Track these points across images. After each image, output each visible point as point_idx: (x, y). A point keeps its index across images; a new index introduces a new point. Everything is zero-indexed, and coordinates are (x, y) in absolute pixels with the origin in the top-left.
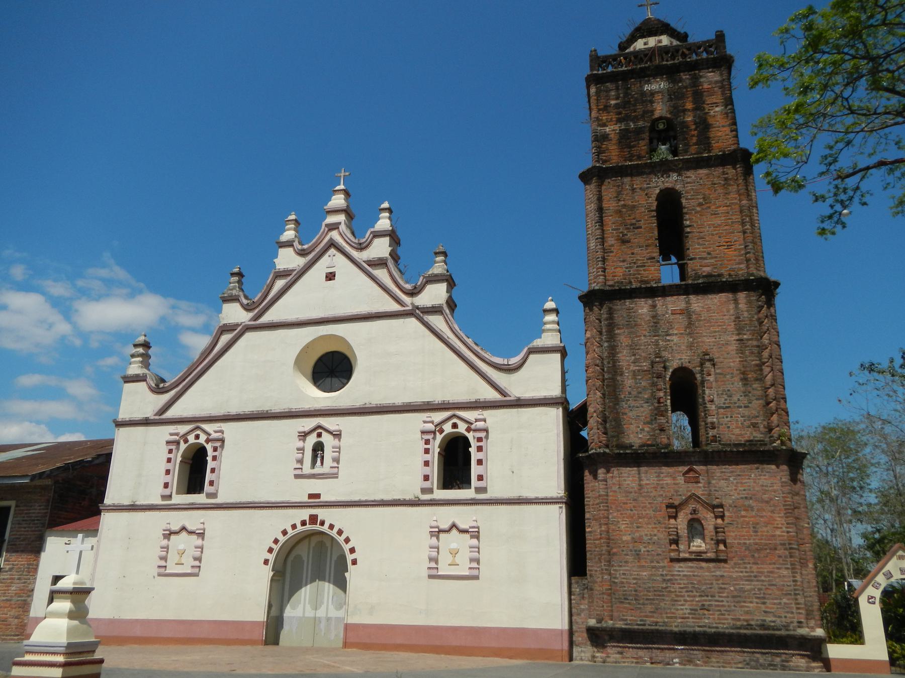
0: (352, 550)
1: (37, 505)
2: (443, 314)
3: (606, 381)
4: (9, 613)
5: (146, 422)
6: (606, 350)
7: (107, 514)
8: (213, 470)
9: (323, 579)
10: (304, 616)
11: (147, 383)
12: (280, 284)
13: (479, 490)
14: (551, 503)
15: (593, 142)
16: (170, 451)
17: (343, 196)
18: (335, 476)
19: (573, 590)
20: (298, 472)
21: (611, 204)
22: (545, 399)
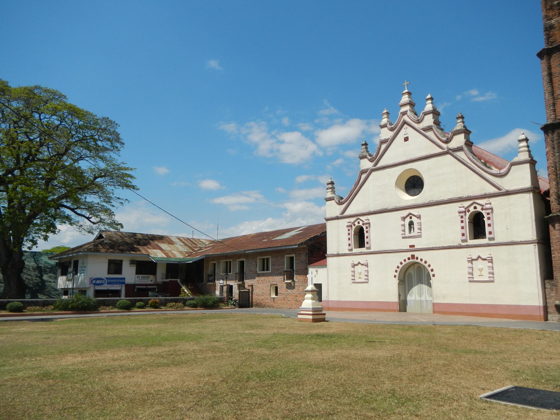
0: (432, 270)
2: (463, 151)
3: (558, 175)
5: (337, 218)
6: (557, 158)
8: (367, 237)
9: (422, 283)
10: (416, 300)
12: (384, 146)
13: (490, 239)
14: (529, 243)
15: (544, 32)
16: (349, 230)
17: (407, 96)
18: (420, 236)
19: (546, 286)
20: (404, 236)
21: (557, 69)
22: (522, 189)
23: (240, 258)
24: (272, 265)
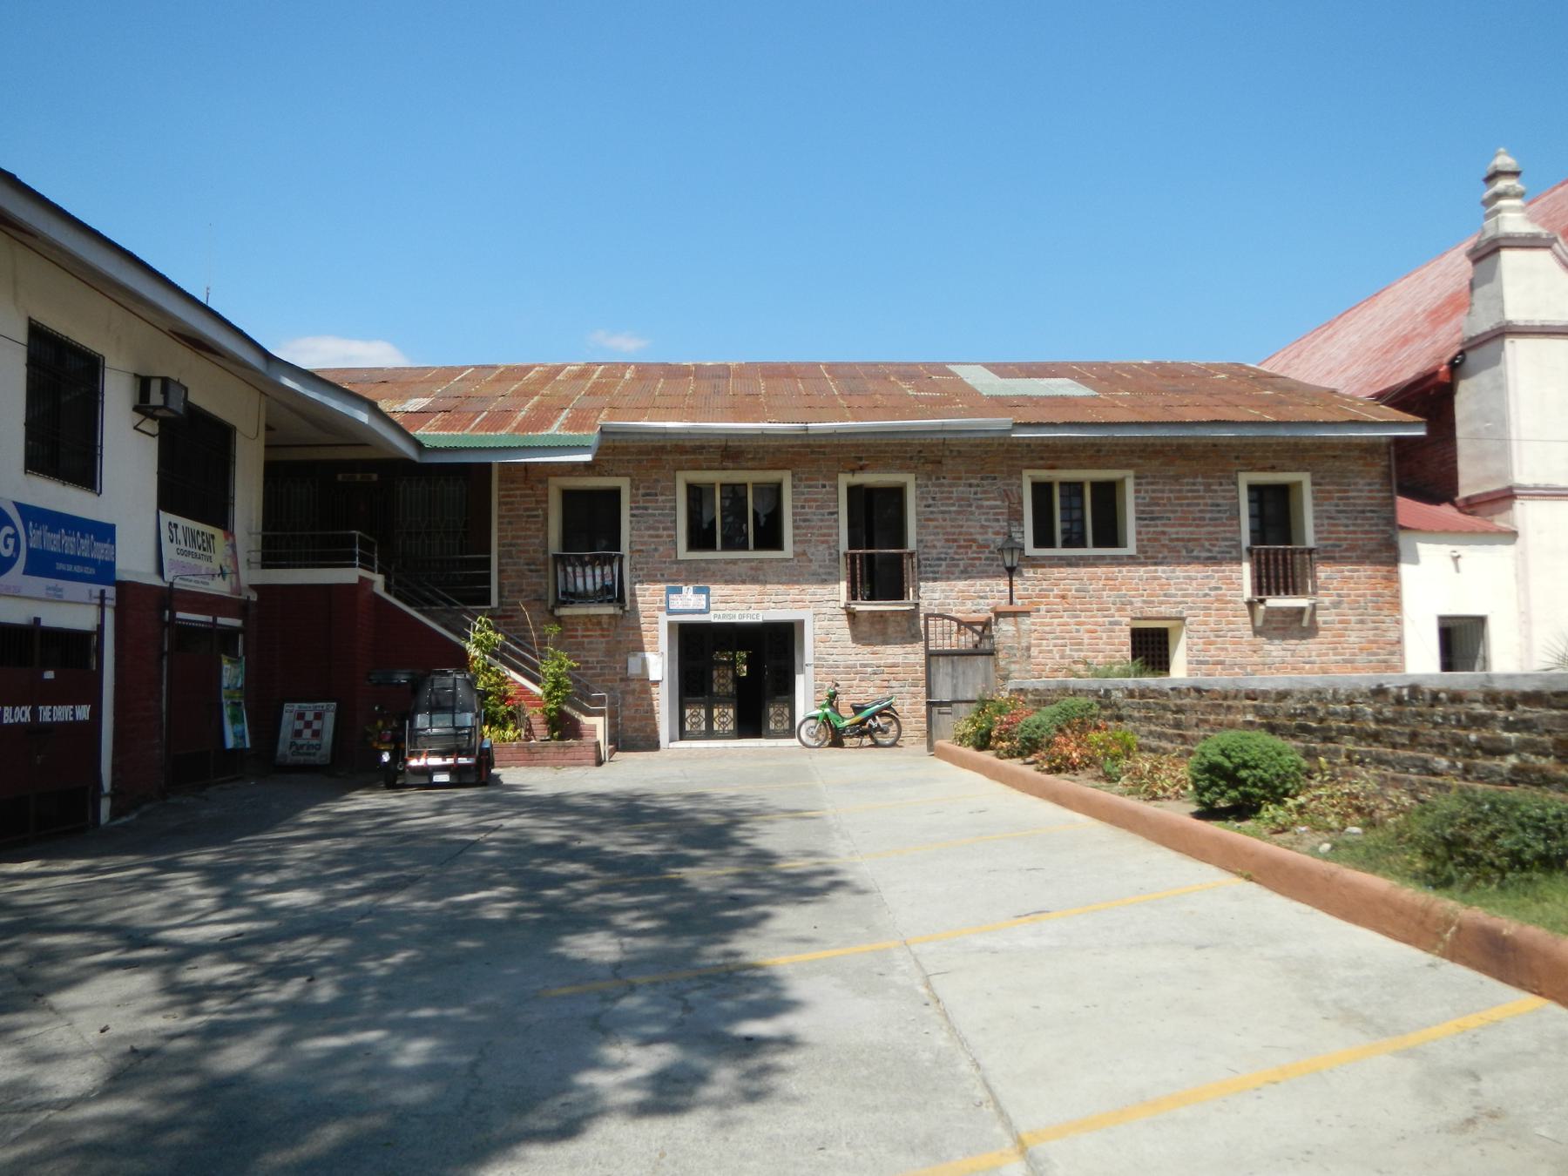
11: (1555, 253)
23: (862, 468)
24: (1138, 519)
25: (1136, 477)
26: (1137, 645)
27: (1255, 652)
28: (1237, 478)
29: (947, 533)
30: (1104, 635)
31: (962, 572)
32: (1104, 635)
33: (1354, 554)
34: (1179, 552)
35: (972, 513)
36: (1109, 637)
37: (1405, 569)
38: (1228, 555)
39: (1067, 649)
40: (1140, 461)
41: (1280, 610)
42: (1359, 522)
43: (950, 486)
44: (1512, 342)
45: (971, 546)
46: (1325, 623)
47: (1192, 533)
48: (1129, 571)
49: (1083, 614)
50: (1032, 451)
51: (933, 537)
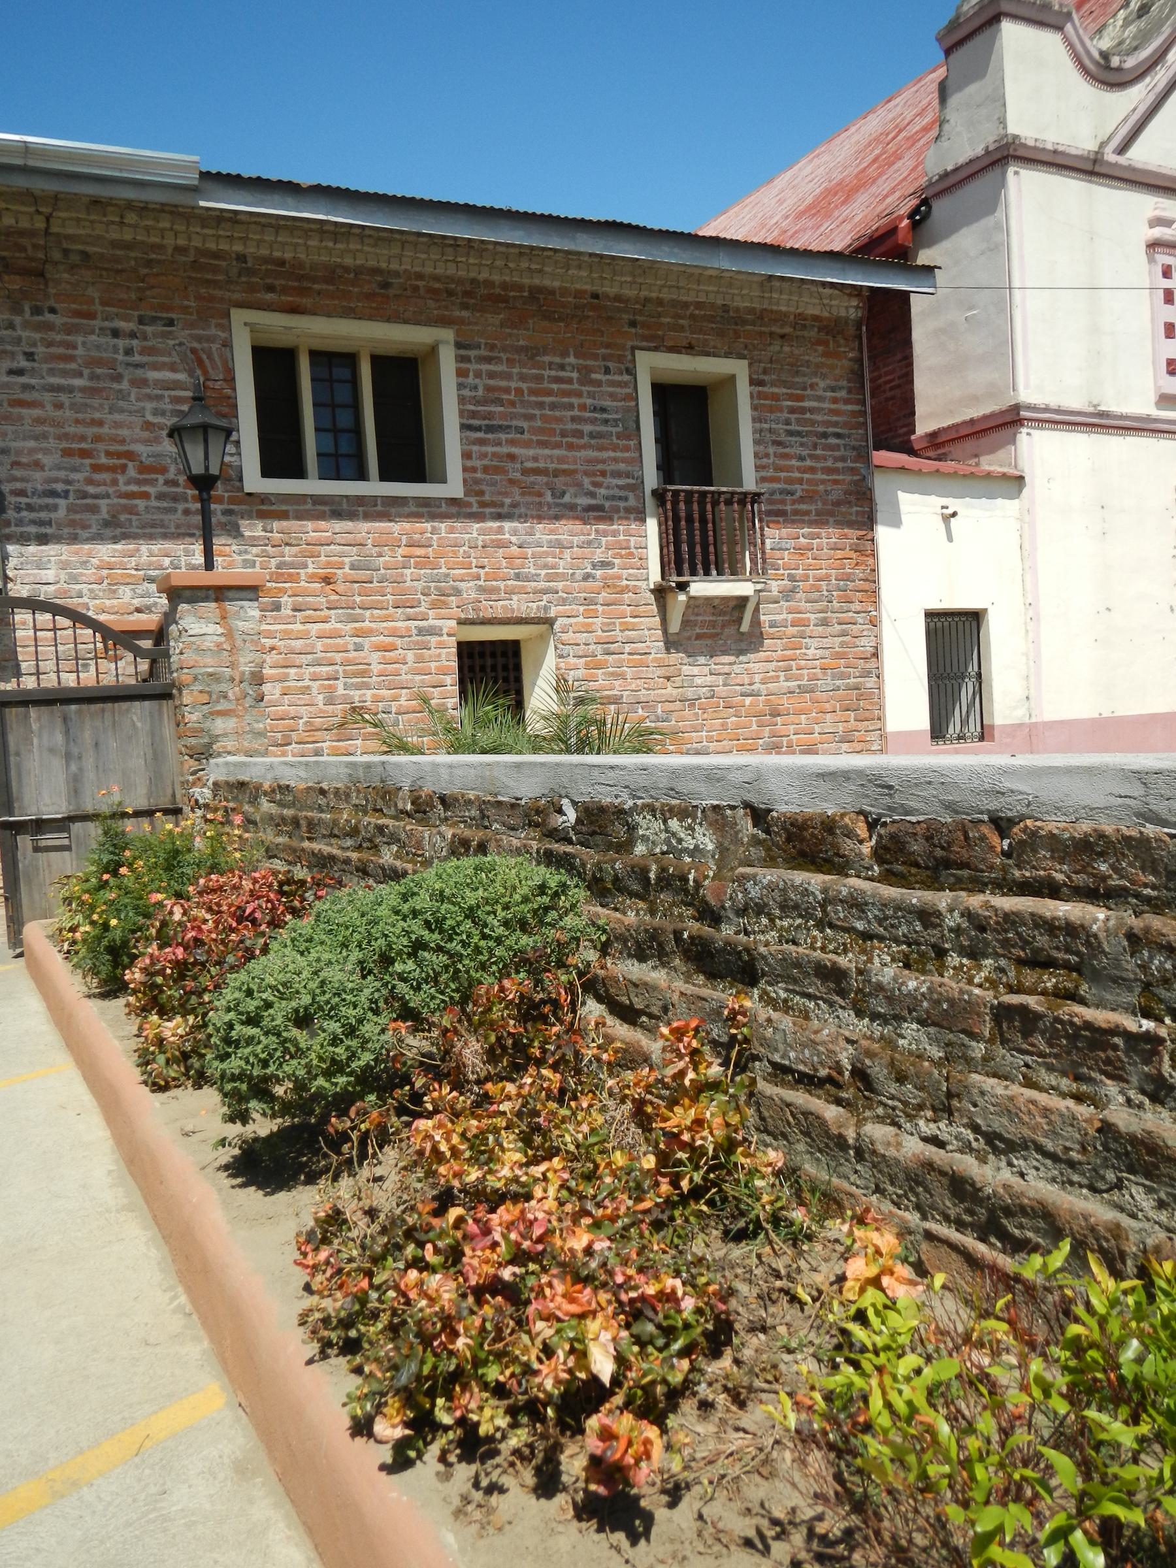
1: (822, 384)
4: (817, 728)
7: (1036, 433)
11: (1066, 39)
24: (464, 427)
25: (459, 345)
26: (467, 675)
27: (668, 679)
28: (634, 361)
29: (66, 437)
30: (410, 656)
31: (107, 524)
32: (410, 656)
33: (813, 507)
34: (540, 495)
35: (122, 395)
36: (419, 660)
37: (883, 533)
38: (622, 504)
39: (340, 684)
40: (465, 314)
41: (708, 600)
42: (818, 452)
43: (69, 330)
44: (1016, 173)
45: (124, 468)
46: (773, 625)
47: (561, 460)
48: (451, 531)
49: (368, 613)
50: (251, 272)
51: (32, 444)
